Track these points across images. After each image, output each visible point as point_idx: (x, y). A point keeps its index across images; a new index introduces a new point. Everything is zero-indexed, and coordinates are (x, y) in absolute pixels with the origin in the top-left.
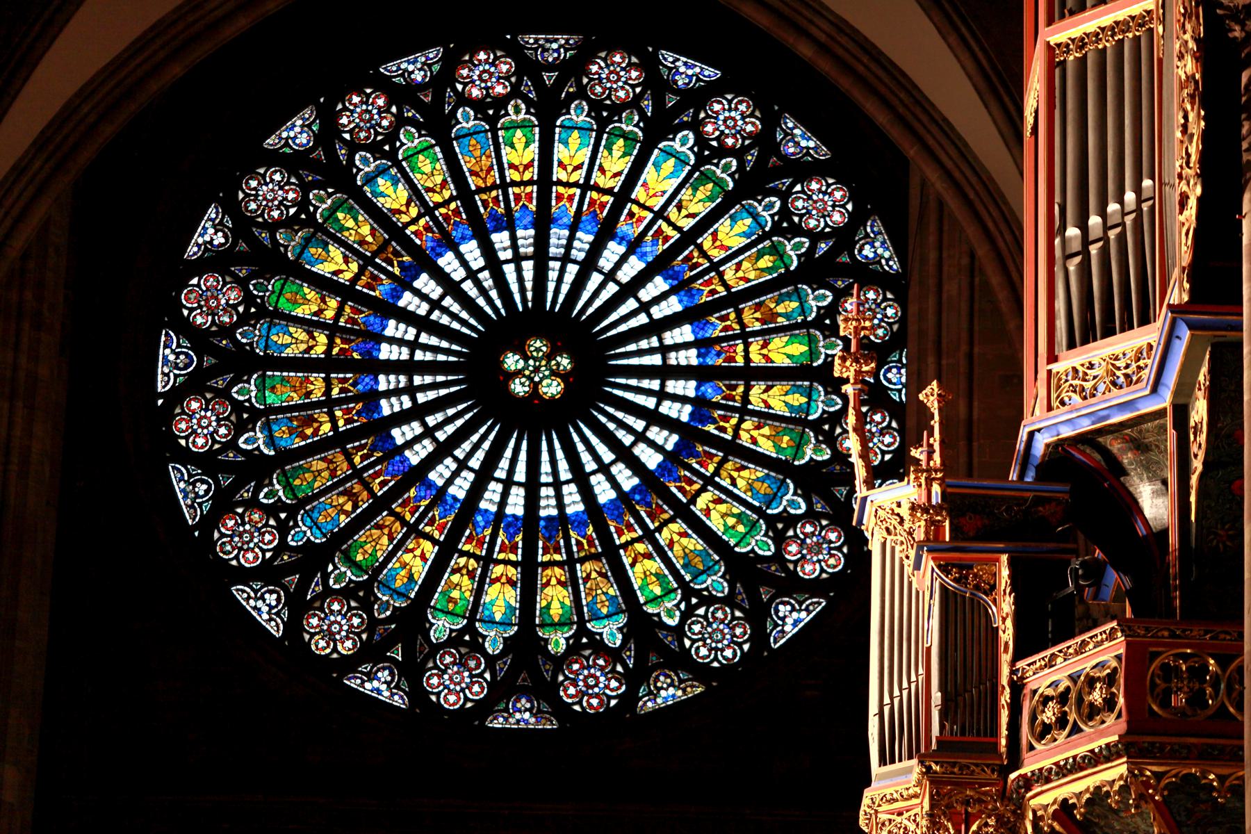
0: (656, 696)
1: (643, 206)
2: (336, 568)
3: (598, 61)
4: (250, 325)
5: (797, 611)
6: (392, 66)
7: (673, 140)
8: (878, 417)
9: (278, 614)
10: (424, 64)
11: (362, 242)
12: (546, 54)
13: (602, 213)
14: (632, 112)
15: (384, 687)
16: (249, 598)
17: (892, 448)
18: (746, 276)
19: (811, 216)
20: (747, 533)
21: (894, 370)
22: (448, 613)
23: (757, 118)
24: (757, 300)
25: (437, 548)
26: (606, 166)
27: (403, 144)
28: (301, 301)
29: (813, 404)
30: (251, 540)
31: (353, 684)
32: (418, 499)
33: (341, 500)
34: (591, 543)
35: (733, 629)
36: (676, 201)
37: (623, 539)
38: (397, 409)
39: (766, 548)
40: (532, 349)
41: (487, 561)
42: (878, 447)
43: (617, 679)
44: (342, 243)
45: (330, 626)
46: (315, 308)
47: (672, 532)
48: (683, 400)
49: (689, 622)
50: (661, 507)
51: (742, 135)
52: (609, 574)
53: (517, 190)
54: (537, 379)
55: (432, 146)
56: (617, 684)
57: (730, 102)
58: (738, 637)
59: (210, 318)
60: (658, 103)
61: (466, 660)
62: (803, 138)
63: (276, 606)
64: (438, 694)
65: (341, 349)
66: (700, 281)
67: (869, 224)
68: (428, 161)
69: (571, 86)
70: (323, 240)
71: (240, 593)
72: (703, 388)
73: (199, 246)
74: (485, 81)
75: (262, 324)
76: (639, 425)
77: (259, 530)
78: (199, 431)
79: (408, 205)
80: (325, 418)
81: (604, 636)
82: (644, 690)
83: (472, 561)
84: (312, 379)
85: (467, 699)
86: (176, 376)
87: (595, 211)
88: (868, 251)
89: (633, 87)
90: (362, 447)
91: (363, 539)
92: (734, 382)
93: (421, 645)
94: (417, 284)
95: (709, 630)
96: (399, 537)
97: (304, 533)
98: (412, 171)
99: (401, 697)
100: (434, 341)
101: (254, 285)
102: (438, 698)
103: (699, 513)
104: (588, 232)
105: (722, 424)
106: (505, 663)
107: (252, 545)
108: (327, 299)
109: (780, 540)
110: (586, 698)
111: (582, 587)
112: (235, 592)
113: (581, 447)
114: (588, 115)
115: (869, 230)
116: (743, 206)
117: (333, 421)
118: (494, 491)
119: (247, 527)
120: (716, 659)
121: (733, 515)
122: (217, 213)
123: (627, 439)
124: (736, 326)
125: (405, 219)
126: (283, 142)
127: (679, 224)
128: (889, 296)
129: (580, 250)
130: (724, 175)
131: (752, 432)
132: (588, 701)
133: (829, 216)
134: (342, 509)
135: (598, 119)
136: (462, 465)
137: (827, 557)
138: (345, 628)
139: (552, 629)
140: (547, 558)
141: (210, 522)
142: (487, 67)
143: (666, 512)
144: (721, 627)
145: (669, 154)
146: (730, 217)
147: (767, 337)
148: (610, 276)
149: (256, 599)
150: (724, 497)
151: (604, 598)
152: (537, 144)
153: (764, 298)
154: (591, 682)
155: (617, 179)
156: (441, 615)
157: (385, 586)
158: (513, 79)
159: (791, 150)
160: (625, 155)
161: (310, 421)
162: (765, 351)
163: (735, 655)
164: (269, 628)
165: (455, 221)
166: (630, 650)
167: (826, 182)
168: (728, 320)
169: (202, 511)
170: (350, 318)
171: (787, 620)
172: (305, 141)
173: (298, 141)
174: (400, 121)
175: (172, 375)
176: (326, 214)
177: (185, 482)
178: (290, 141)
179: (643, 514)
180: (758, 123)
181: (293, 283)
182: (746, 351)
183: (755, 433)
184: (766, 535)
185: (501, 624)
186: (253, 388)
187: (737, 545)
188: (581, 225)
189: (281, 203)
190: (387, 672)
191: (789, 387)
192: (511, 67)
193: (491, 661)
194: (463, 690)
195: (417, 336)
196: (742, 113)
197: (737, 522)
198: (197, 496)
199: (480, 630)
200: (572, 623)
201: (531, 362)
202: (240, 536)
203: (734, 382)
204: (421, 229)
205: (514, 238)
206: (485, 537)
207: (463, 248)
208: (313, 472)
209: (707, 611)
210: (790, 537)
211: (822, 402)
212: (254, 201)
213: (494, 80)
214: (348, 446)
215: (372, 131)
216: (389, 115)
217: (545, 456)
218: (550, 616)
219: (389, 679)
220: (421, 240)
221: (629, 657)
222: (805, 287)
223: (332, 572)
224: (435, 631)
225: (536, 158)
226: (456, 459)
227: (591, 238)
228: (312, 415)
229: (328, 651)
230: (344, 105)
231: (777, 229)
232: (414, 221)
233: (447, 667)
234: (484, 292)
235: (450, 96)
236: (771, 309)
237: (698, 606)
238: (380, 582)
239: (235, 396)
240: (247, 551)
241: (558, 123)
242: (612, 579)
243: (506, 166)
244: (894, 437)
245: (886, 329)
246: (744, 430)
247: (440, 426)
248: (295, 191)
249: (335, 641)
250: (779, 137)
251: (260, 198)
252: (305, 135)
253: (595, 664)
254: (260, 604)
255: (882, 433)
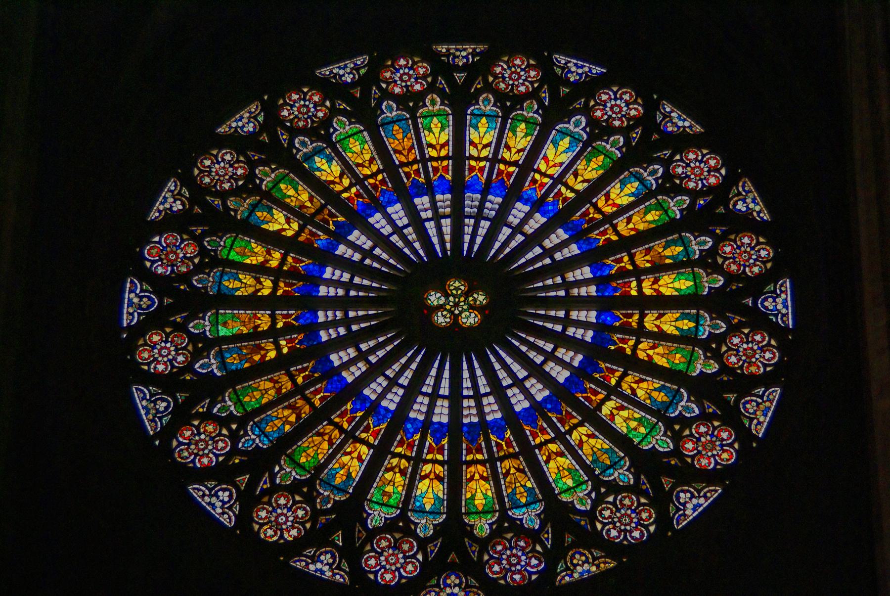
0: (573, 572)
1: (544, 175)
2: (281, 469)
3: (502, 64)
4: (204, 273)
5: (695, 497)
6: (325, 71)
7: (569, 122)
8: (758, 338)
9: (230, 508)
10: (352, 69)
11: (303, 207)
12: (456, 60)
13: (509, 180)
14: (532, 102)
15: (326, 568)
16: (204, 495)
17: (772, 362)
18: (636, 227)
19: (690, 180)
20: (647, 434)
21: (770, 300)
22: (383, 505)
23: (639, 104)
24: (647, 246)
25: (372, 451)
26: (511, 143)
27: (336, 130)
28: (249, 254)
29: (701, 328)
30: (206, 448)
31: (300, 565)
32: (354, 411)
33: (286, 413)
34: (509, 444)
35: (640, 513)
36: (573, 170)
37: (538, 441)
38: (334, 336)
39: (665, 446)
40: (452, 288)
41: (418, 461)
42: (760, 361)
43: (536, 558)
44: (284, 206)
45: (277, 518)
46: (261, 259)
47: (581, 435)
48: (585, 325)
49: (600, 508)
50: (570, 413)
51: (626, 118)
52: (526, 469)
53: (435, 164)
54: (457, 312)
55: (361, 131)
56: (537, 562)
57: (615, 93)
58: (644, 521)
59: (169, 269)
60: (554, 94)
61: (400, 544)
62: (680, 120)
63: (229, 502)
64: (376, 573)
65: (285, 291)
66: (597, 232)
67: (741, 184)
68: (357, 143)
69: (479, 83)
70: (267, 206)
71: (196, 491)
72: (603, 317)
73: (160, 212)
74: (406, 82)
75: (216, 273)
76: (549, 347)
77: (212, 438)
78: (160, 359)
79: (341, 176)
80: (270, 346)
81: (524, 522)
82: (562, 566)
83: (403, 461)
84: (259, 315)
85: (401, 576)
86: (139, 314)
87: (503, 179)
88: (740, 206)
89: (532, 83)
90: (304, 370)
91: (306, 445)
92: (629, 312)
93: (359, 532)
94: (351, 238)
95: (618, 515)
96: (338, 443)
97: (252, 439)
98: (344, 151)
99: (342, 576)
100: (366, 282)
101: (207, 241)
102: (376, 577)
103: (605, 418)
104: (497, 196)
105: (621, 345)
106: (435, 546)
107: (206, 451)
108: (272, 252)
109: (677, 438)
110: (509, 574)
111: (502, 482)
112: (191, 491)
113: (497, 366)
114: (495, 105)
115: (741, 189)
116: (631, 173)
117: (278, 348)
118: (421, 404)
119: (203, 437)
120: (625, 538)
121: (635, 419)
122: (176, 186)
123: (539, 359)
124: (630, 267)
125: (338, 188)
126: (233, 130)
127: (576, 188)
128: (761, 240)
129: (491, 210)
130: (613, 149)
131: (648, 352)
132: (511, 577)
133: (705, 179)
134: (286, 421)
135: (503, 108)
136: (393, 382)
137: (720, 453)
138: (291, 519)
139: (476, 517)
140: (470, 457)
141: (169, 432)
142: (407, 70)
143: (575, 418)
144: (629, 512)
145: (564, 133)
146: (620, 181)
147: (657, 275)
148: (517, 229)
149: (210, 496)
150: (626, 405)
151: (522, 490)
152: (451, 128)
153: (653, 244)
154: (514, 560)
155: (521, 154)
156: (377, 507)
157: (328, 484)
158: (429, 79)
159: (670, 129)
160: (526, 135)
161: (259, 348)
162: (656, 286)
163: (642, 536)
164: (223, 520)
165: (382, 189)
166: (547, 532)
167: (702, 152)
168: (623, 262)
169: (162, 424)
170: (292, 266)
171: (688, 505)
172: (251, 129)
173: (245, 129)
174: (334, 112)
175: (136, 314)
176: (270, 185)
177: (147, 400)
178: (239, 129)
179: (555, 420)
180: (640, 108)
181: (242, 239)
182: (640, 287)
183: (650, 352)
184: (665, 434)
185: (431, 513)
186: (207, 323)
187: (639, 443)
188: (492, 191)
189: (231, 177)
190: (329, 556)
191: (678, 315)
192: (427, 69)
193: (423, 543)
194: (398, 569)
195: (352, 279)
196: (626, 101)
197: (638, 425)
198: (158, 411)
199: (413, 519)
200: (495, 511)
201: (451, 299)
202: (196, 444)
203: (629, 312)
204: (353, 195)
205: (434, 203)
206: (414, 441)
207: (390, 210)
208: (261, 390)
209: (615, 499)
210: (687, 436)
211: (708, 326)
212: (208, 176)
213: (413, 80)
214: (292, 369)
215: (309, 120)
216: (324, 108)
217: (466, 374)
218: (474, 505)
219: (331, 561)
220: (353, 205)
221: (547, 539)
222: (687, 234)
223: (279, 472)
224: (372, 521)
225: (451, 138)
226: (387, 377)
227: (500, 200)
228: (259, 344)
229: (275, 538)
230: (284, 101)
231: (661, 190)
232: (347, 190)
233: (383, 550)
234: (409, 244)
235: (375, 93)
236: (659, 253)
237: (607, 494)
238: (321, 480)
239: (192, 330)
240: (202, 456)
241: (469, 112)
242: (529, 474)
243: (425, 145)
244: (773, 353)
245: (761, 267)
246: (641, 350)
247: (372, 351)
248: (244, 168)
249: (282, 530)
250: (659, 118)
251: (213, 174)
252: (251, 125)
253: (517, 545)
254: (214, 500)
255: (762, 349)
